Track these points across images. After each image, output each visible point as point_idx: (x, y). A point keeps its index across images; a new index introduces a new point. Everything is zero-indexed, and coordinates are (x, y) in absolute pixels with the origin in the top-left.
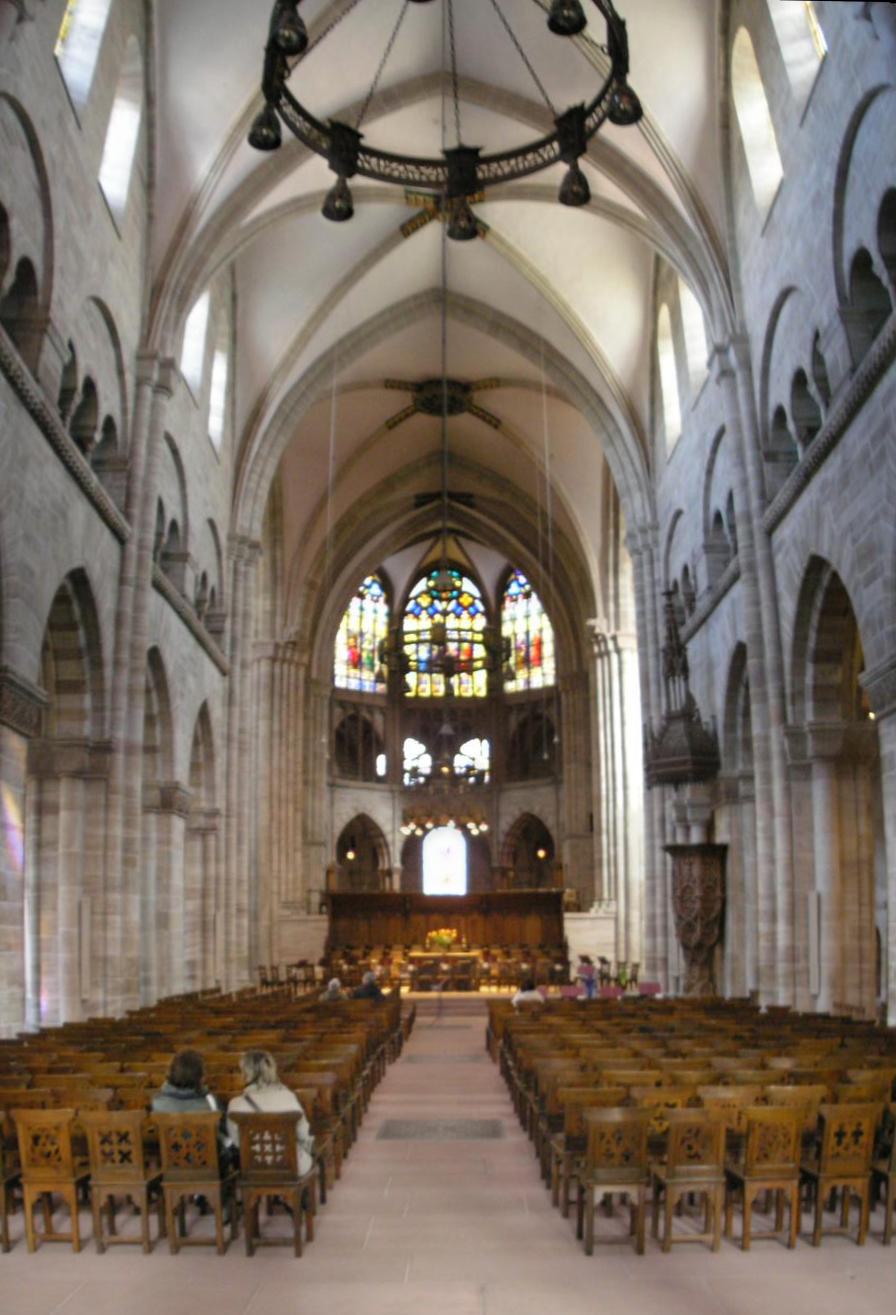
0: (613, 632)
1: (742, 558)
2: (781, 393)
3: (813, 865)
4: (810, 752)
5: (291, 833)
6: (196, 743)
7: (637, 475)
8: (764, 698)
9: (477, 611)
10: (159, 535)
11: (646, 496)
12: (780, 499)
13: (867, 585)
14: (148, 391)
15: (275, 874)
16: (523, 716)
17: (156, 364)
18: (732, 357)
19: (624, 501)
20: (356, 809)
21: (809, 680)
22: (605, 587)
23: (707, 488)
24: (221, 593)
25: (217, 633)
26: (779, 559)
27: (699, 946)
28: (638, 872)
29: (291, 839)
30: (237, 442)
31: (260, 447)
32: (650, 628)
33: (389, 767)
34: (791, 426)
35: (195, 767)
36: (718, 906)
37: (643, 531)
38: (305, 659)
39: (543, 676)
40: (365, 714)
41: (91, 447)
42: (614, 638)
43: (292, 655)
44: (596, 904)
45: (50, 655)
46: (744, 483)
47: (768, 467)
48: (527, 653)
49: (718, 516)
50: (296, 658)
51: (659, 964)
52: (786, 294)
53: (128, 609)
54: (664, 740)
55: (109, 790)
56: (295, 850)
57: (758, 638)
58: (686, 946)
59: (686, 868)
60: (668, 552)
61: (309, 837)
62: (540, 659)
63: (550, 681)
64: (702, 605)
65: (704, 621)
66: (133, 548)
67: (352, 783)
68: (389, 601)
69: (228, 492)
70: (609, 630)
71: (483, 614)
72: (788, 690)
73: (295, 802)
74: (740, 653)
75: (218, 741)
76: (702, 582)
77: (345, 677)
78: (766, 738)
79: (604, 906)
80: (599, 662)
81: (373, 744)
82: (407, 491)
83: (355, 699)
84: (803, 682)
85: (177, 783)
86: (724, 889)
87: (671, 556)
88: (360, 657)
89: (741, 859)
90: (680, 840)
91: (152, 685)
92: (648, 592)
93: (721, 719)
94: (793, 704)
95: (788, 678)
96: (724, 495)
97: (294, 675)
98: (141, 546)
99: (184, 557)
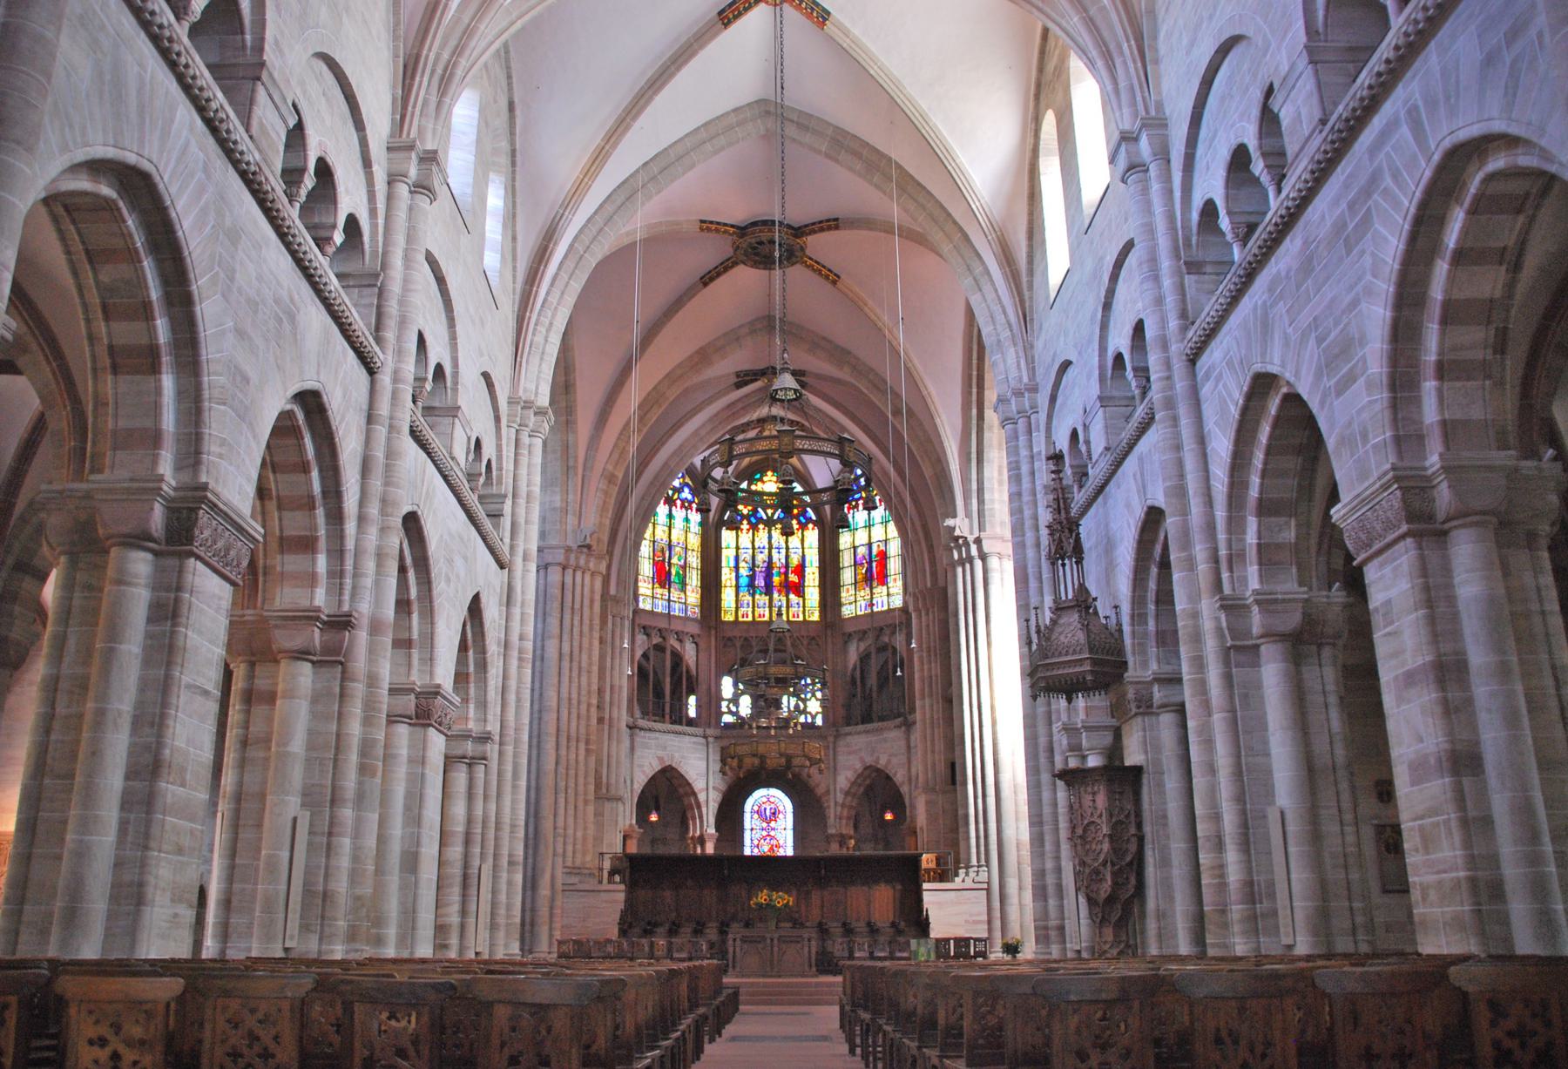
0: (976, 534)
1: (1155, 394)
2: (1211, 183)
3: (1269, 772)
4: (1256, 629)
5: (581, 780)
6: (463, 647)
7: (1010, 326)
8: (1190, 564)
9: (809, 520)
10: (420, 380)
11: (1022, 354)
12: (1209, 309)
13: (1339, 394)
14: (403, 190)
15: (561, 831)
16: (863, 646)
17: (413, 155)
18: (1144, 146)
19: (991, 358)
20: (661, 759)
21: (1251, 538)
22: (966, 480)
23: (1104, 326)
24: (500, 469)
25: (495, 516)
26: (1206, 390)
27: (1111, 900)
28: (1018, 829)
29: (581, 788)
30: (519, 286)
31: (548, 294)
32: (1027, 513)
33: (698, 707)
34: (1224, 223)
35: (461, 678)
36: (1133, 847)
37: (1018, 393)
38: (603, 567)
39: (890, 596)
40: (673, 642)
41: (330, 250)
42: (978, 541)
43: (587, 562)
44: (962, 872)
45: (272, 506)
46: (1159, 301)
47: (1189, 280)
48: (869, 569)
49: (1119, 358)
50: (591, 565)
51: (1053, 934)
52: (1224, 49)
53: (379, 454)
54: (1054, 637)
55: (345, 677)
56: (586, 802)
57: (1179, 491)
58: (1091, 902)
59: (1087, 799)
60: (1050, 417)
61: (604, 791)
62: (883, 579)
63: (897, 602)
64: (1095, 473)
65: (1100, 490)
66: (385, 379)
67: (659, 726)
68: (704, 510)
69: (510, 350)
70: (971, 533)
71: (815, 523)
72: (1223, 552)
73: (587, 742)
74: (1154, 517)
75: (493, 648)
76: (1098, 446)
77: (649, 596)
78: (1195, 615)
80: (960, 570)
81: (685, 682)
82: (727, 366)
83: (663, 624)
84: (1243, 540)
85: (439, 686)
86: (1139, 826)
87: (1055, 422)
88: (669, 573)
89: (1160, 785)
90: (1073, 763)
91: (409, 560)
92: (1025, 469)
93: (1126, 609)
94: (1231, 569)
95: (1222, 536)
96: (1128, 330)
97: (588, 586)
98: (396, 379)
99: (453, 411)
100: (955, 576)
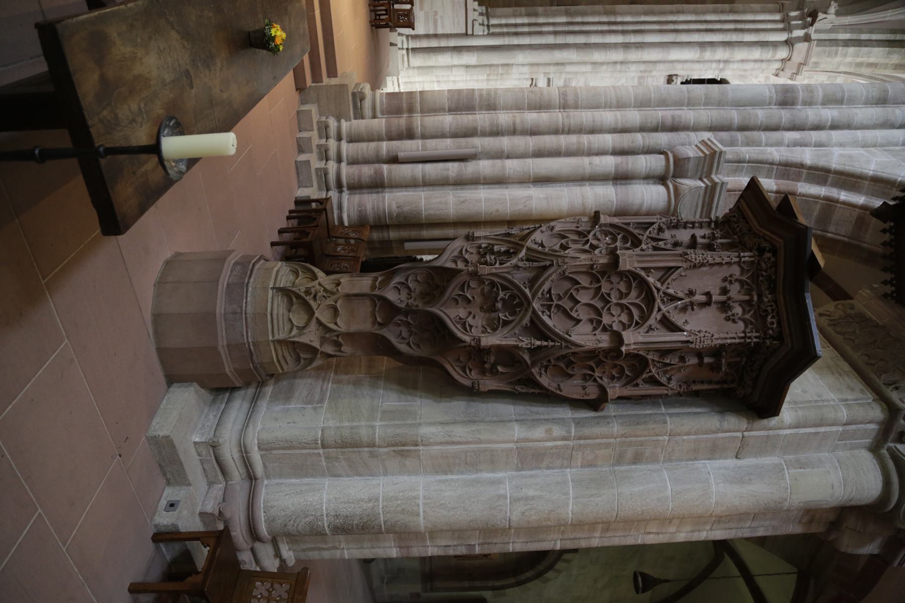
0: (814, 36)
42: (807, 38)
70: (816, 31)
79: (480, 19)
80: (778, 17)
100: (770, 12)
